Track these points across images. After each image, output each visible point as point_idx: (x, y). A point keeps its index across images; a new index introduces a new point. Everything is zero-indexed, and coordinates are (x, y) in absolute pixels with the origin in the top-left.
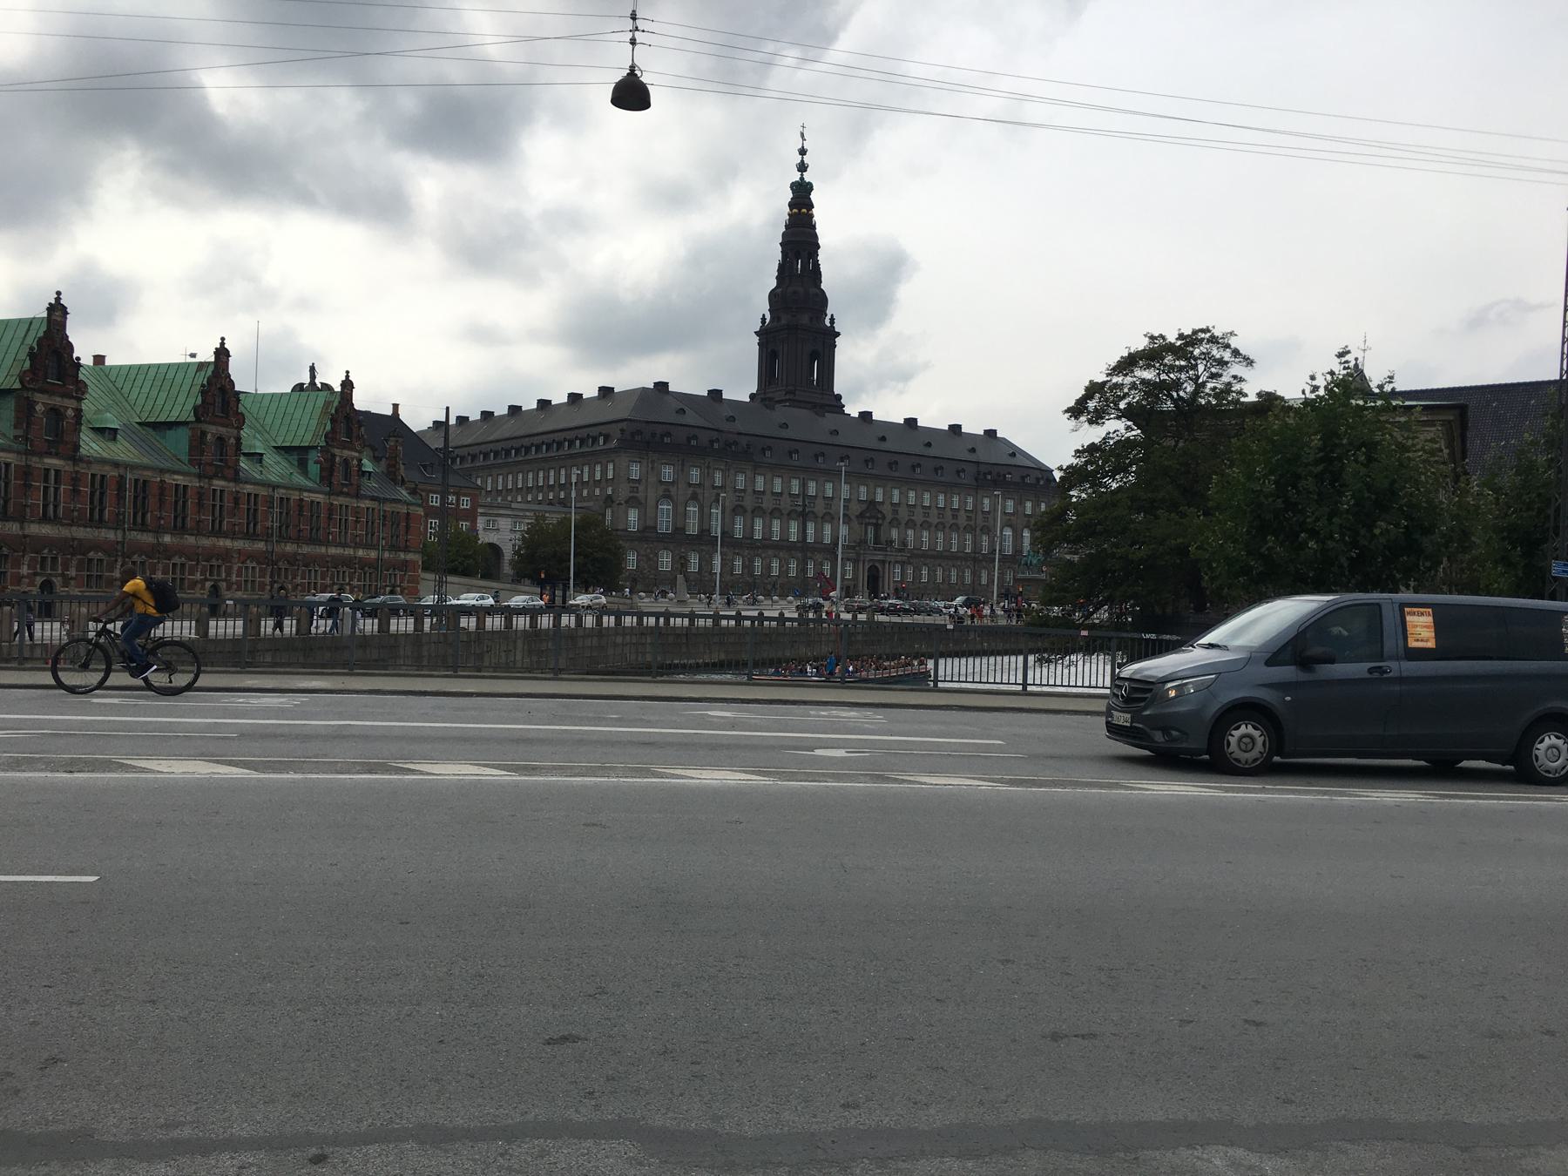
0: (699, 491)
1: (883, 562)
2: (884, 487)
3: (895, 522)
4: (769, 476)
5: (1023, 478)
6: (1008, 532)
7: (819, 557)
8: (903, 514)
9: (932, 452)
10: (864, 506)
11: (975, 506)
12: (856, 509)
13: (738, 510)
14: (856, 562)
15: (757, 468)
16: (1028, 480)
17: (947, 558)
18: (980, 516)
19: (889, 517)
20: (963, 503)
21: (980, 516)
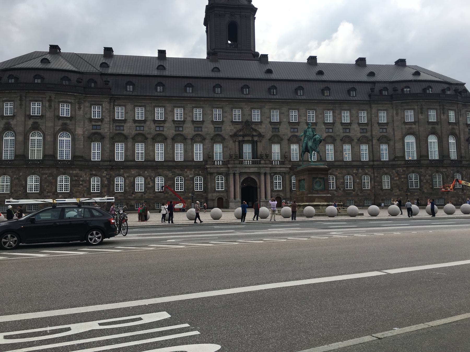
0: (39, 121)
1: (259, 174)
2: (261, 109)
3: (276, 138)
4: (129, 106)
5: (424, 90)
6: (410, 140)
7: (190, 174)
8: (285, 130)
9: (324, 78)
10: (239, 127)
11: (370, 120)
12: (228, 129)
13: (95, 136)
14: (227, 175)
15: (115, 100)
16: (430, 91)
17: (340, 167)
18: (376, 127)
19: (269, 135)
20: (354, 117)
21: (376, 127)
